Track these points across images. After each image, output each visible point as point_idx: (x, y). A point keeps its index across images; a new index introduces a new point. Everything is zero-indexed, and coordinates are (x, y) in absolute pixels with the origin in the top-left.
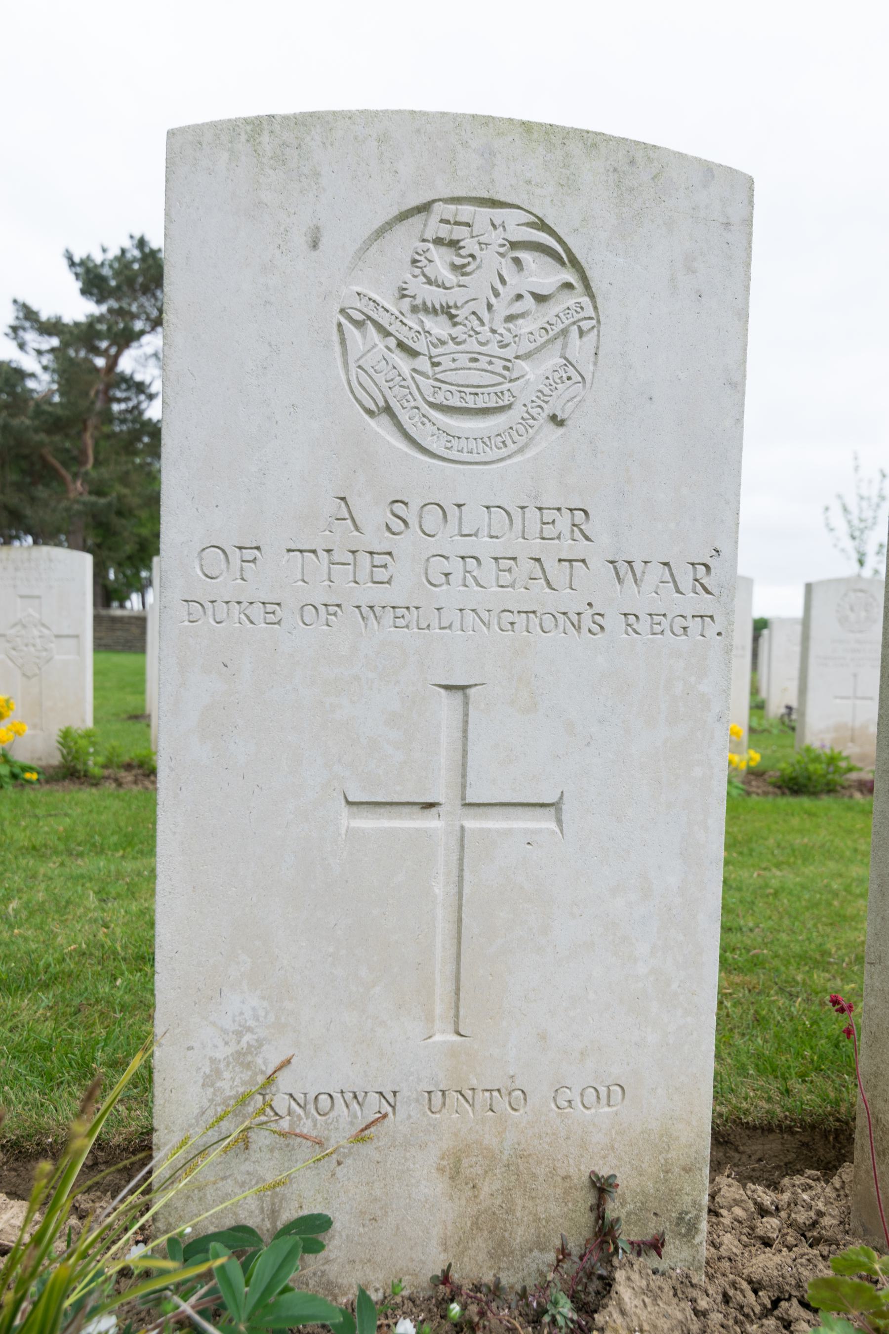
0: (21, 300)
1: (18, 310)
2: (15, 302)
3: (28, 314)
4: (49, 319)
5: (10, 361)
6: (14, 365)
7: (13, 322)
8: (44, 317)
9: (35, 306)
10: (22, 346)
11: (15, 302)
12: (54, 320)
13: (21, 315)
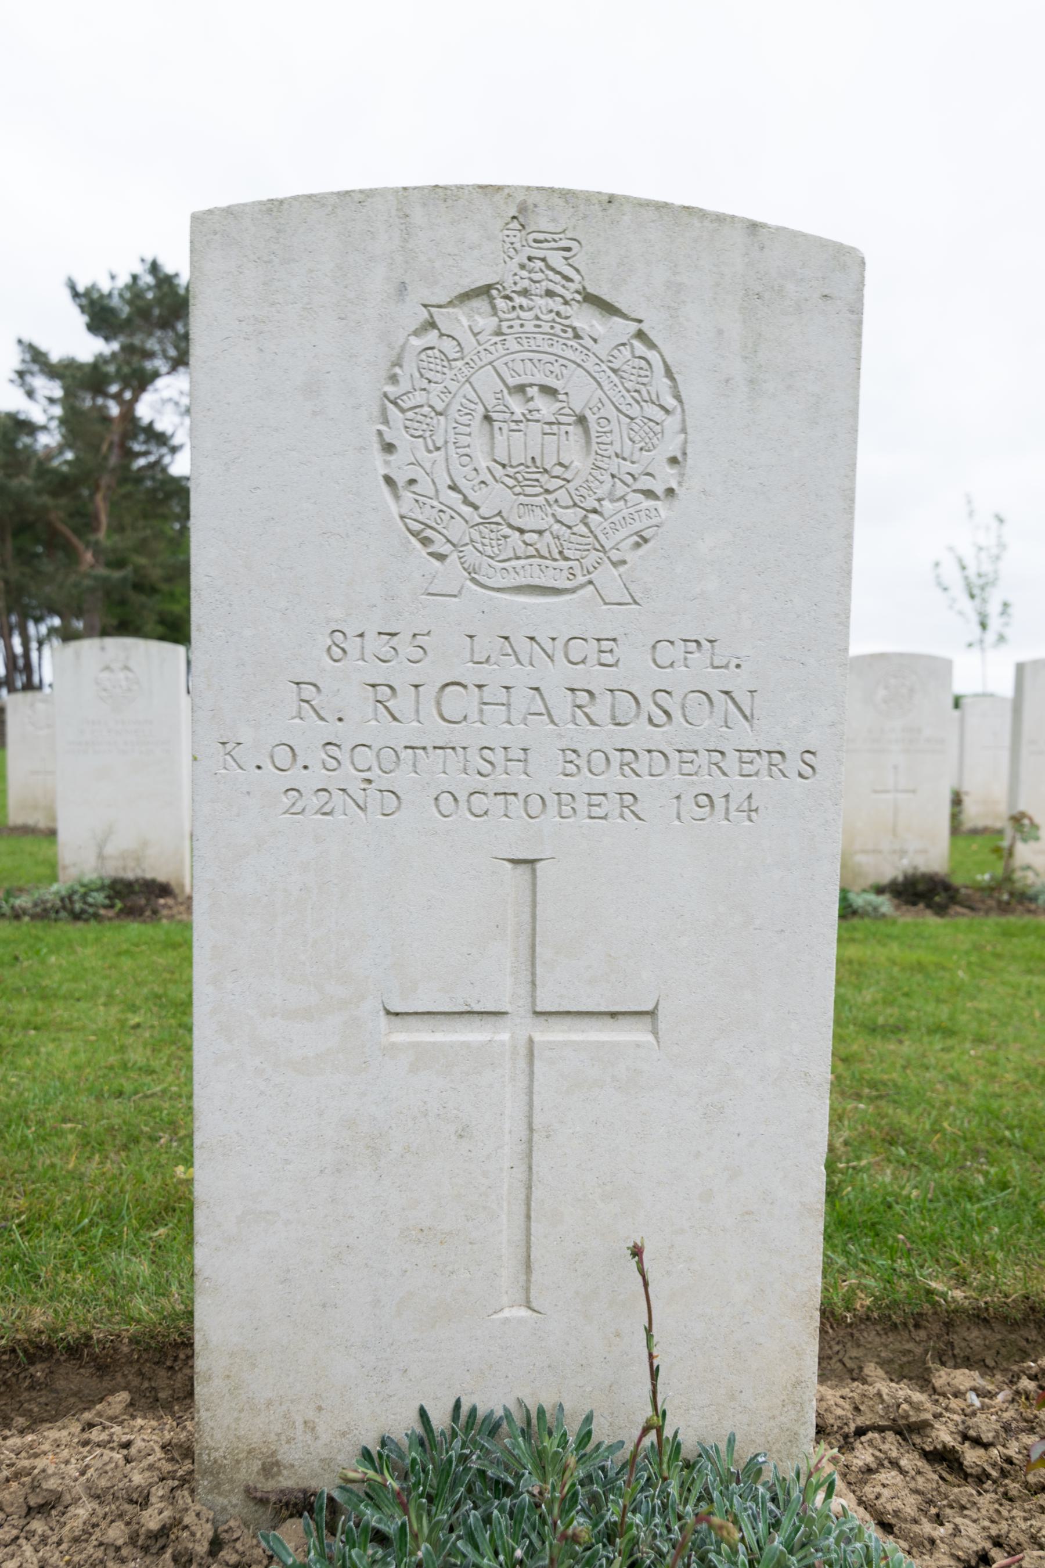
0: (27, 338)
1: (23, 352)
2: (20, 342)
3: (36, 357)
4: (61, 361)
5: (18, 413)
6: (22, 417)
7: (19, 366)
8: (55, 357)
9: (43, 346)
10: (30, 394)
11: (20, 342)
12: (66, 363)
13: (28, 357)
